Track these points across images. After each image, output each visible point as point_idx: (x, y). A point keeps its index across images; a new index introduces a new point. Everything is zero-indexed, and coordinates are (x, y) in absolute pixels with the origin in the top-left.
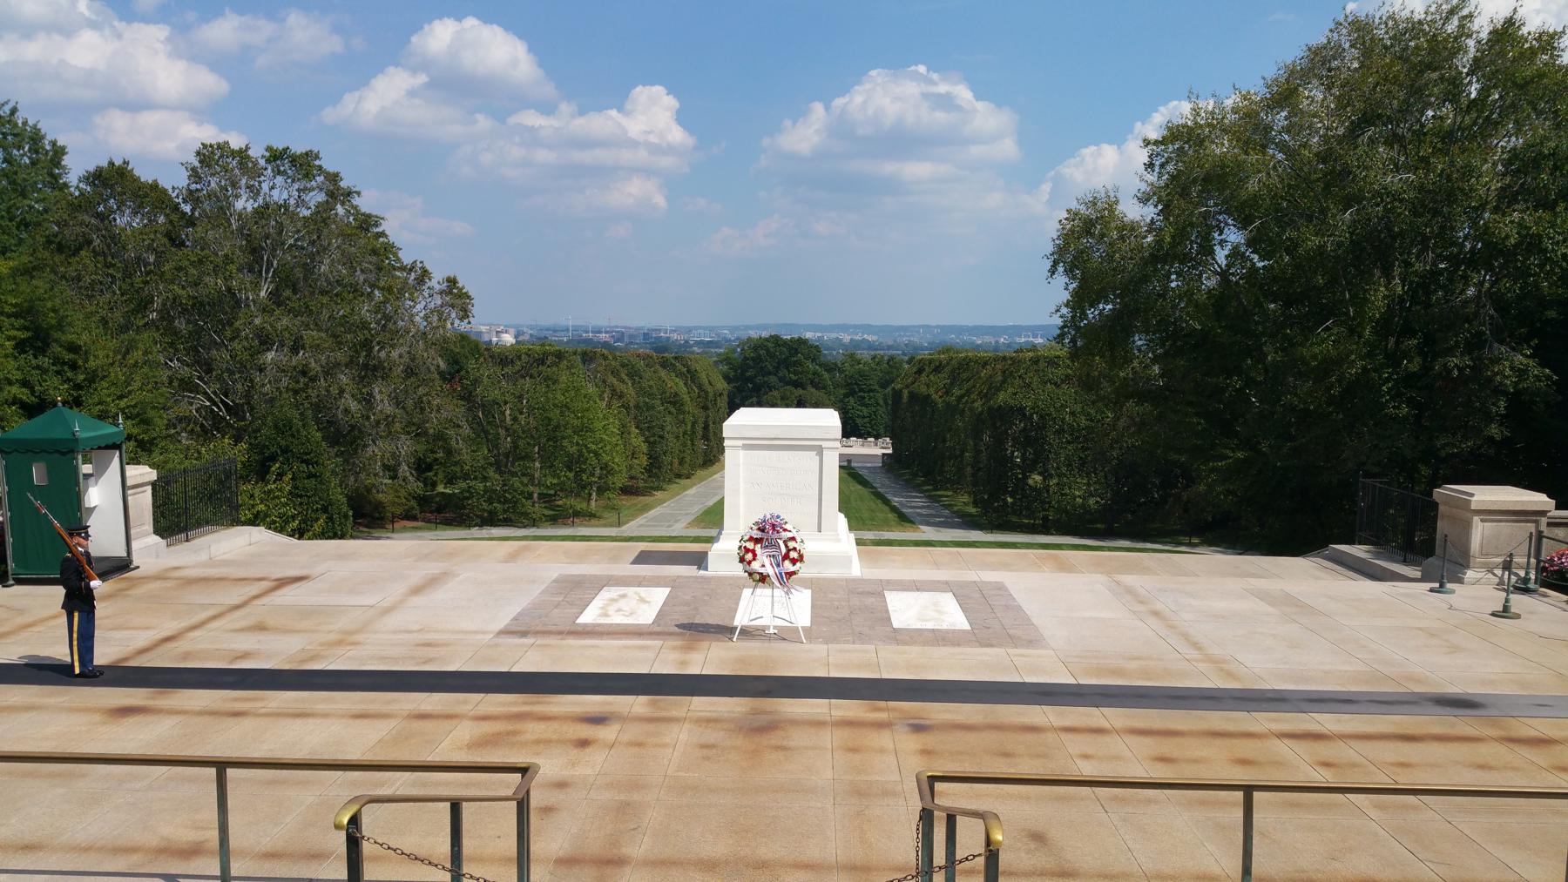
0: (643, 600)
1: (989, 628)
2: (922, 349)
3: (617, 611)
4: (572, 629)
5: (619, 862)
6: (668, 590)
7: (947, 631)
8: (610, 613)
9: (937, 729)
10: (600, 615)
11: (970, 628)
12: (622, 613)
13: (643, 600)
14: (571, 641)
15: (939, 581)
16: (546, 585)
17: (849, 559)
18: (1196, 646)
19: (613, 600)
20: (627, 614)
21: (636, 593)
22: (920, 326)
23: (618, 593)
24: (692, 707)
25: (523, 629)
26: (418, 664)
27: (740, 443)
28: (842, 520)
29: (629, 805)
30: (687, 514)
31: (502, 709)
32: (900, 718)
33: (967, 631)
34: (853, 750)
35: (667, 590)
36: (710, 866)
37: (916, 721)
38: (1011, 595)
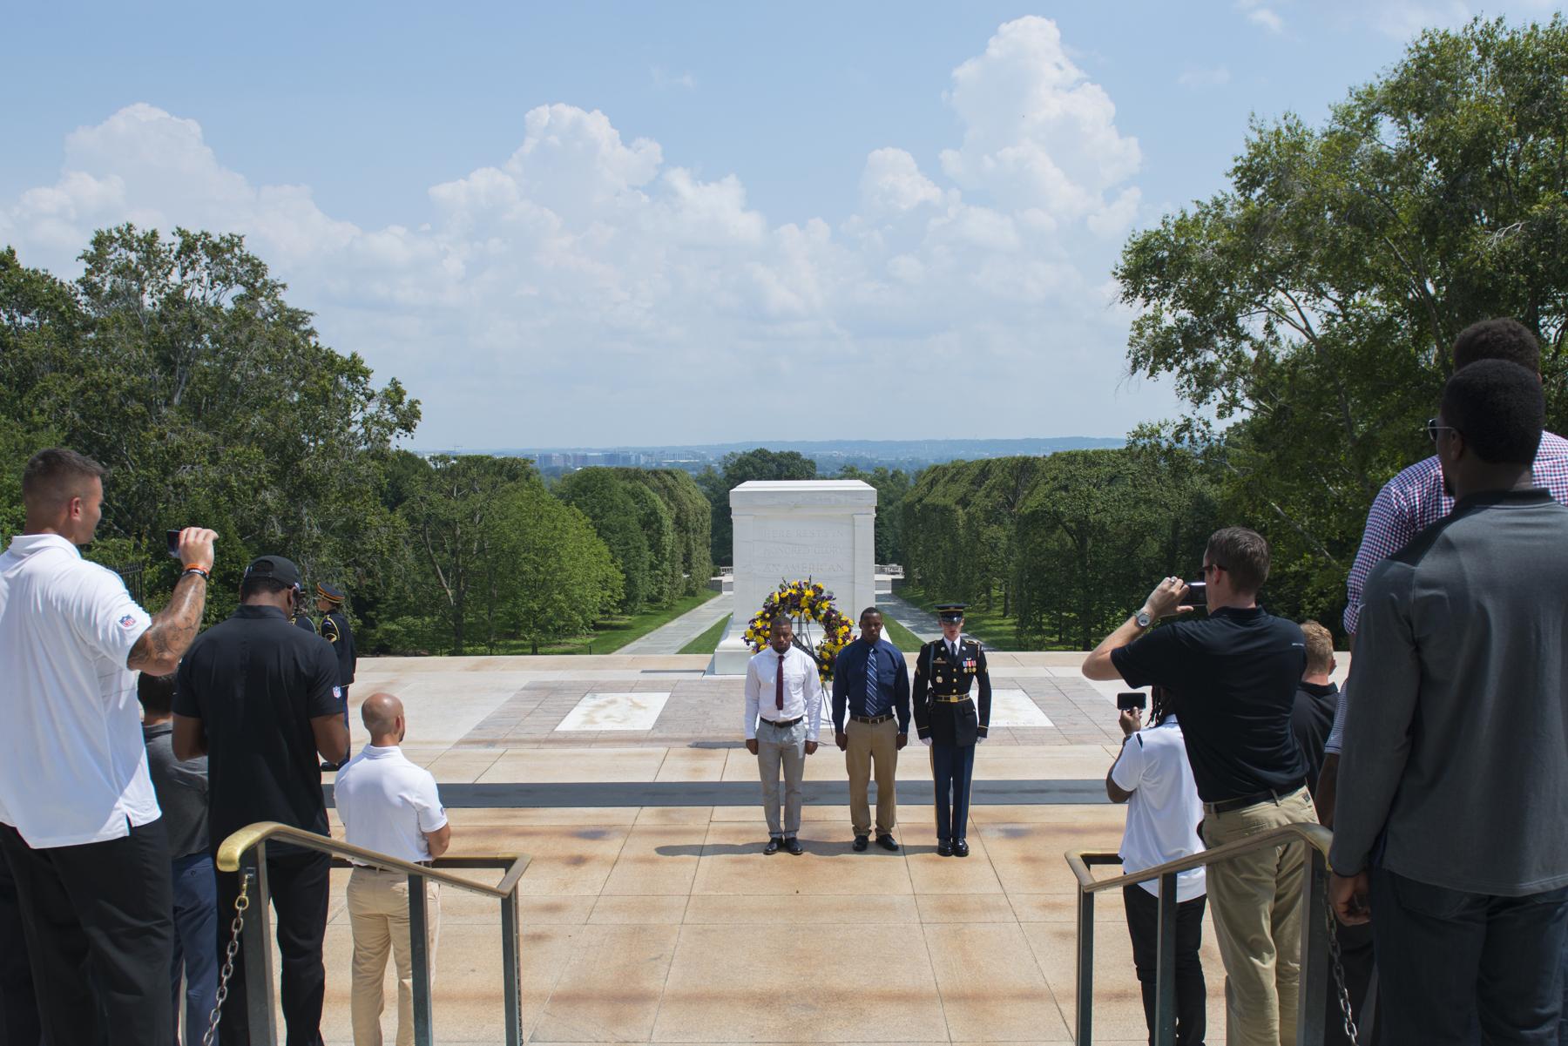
0: (636, 706)
1: (1076, 724)
3: (606, 718)
4: (552, 736)
5: (641, 998)
6: (667, 695)
7: (1025, 729)
8: (598, 720)
9: (1038, 834)
10: (585, 722)
13: (636, 706)
21: (627, 699)
24: (714, 818)
25: (490, 737)
29: (644, 930)
31: (468, 824)
32: (987, 823)
33: (1051, 729)
35: (667, 695)
36: (767, 1001)
37: (1009, 826)
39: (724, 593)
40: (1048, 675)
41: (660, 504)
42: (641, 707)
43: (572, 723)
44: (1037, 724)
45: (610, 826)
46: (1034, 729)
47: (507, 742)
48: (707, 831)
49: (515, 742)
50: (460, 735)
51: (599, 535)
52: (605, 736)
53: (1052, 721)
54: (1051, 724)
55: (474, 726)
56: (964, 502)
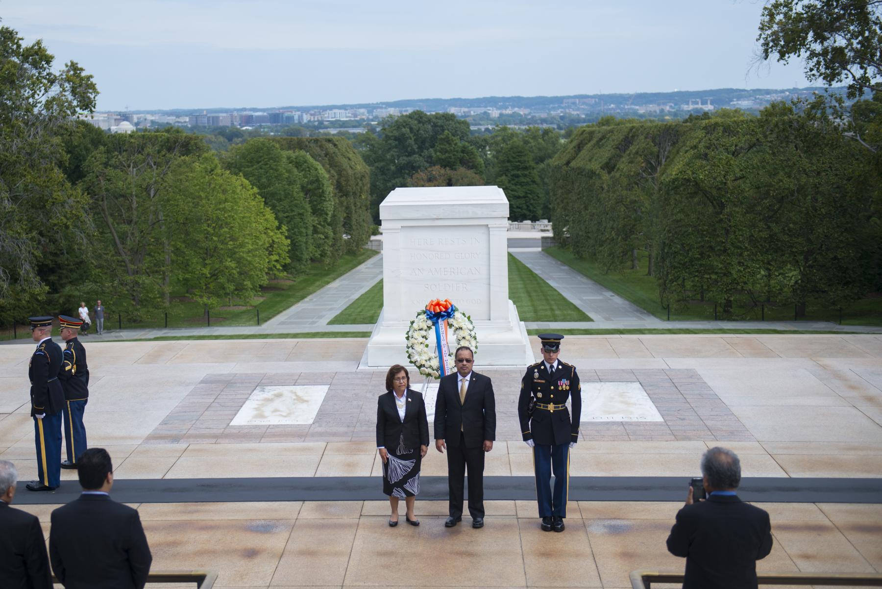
1: (684, 419)
2: (579, 121)
4: (227, 431)
6: (326, 388)
7: (638, 424)
8: (266, 414)
10: (256, 417)
11: (662, 420)
12: (278, 413)
14: (226, 445)
15: (623, 370)
16: (193, 387)
17: (522, 349)
20: (284, 414)
21: (292, 392)
22: (575, 97)
23: (273, 393)
24: (364, 512)
25: (174, 433)
28: (512, 309)
30: (331, 309)
31: (159, 519)
33: (660, 424)
34: (547, 554)
35: (326, 388)
37: (613, 522)
38: (705, 383)
40: (665, 367)
41: (322, 171)
43: (244, 418)
44: (649, 419)
45: (278, 520)
46: (645, 424)
47: (190, 437)
48: (358, 525)
49: (196, 437)
50: (148, 429)
51: (266, 203)
52: (273, 430)
53: (663, 416)
54: (659, 419)
55: (160, 421)
56: (609, 167)
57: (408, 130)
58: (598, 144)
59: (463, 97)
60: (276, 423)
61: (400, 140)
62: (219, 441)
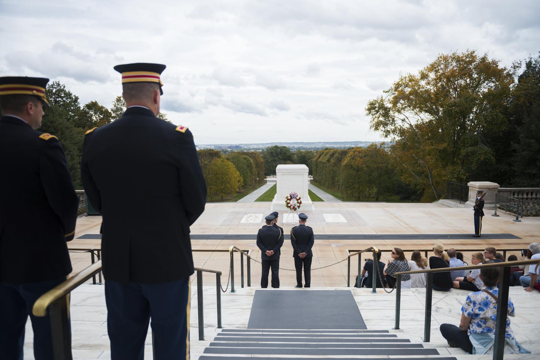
6: (263, 214)
7: (341, 223)
18: (407, 224)
19: (248, 217)
21: (254, 215)
22: (318, 142)
26: (201, 233)
27: (281, 174)
34: (322, 251)
39: (267, 183)
41: (252, 161)
42: (258, 217)
43: (243, 221)
53: (347, 221)
54: (347, 222)
56: (329, 161)
57: (274, 151)
58: (325, 155)
59: (288, 142)
60: (252, 222)
61: (272, 153)
62: (238, 226)
